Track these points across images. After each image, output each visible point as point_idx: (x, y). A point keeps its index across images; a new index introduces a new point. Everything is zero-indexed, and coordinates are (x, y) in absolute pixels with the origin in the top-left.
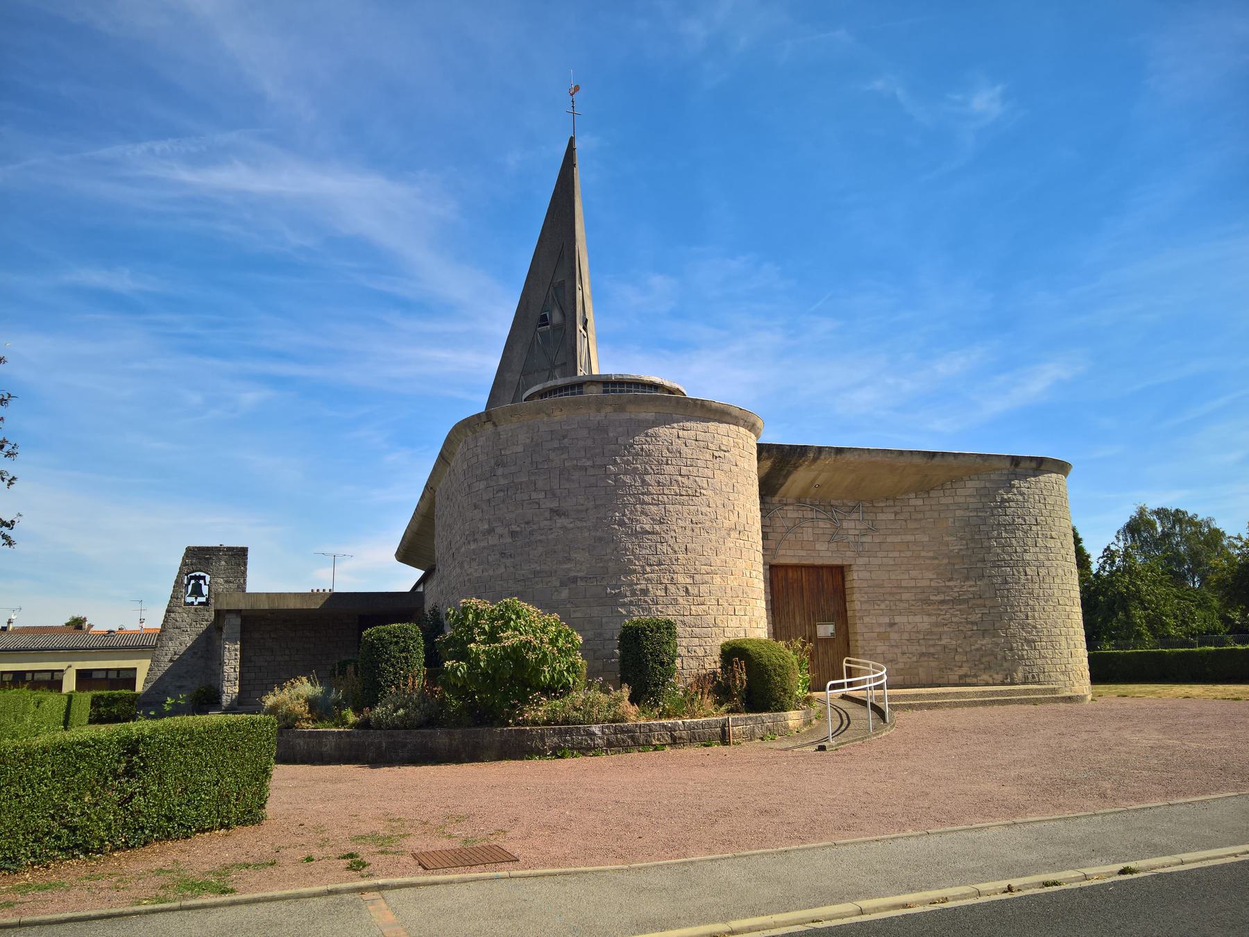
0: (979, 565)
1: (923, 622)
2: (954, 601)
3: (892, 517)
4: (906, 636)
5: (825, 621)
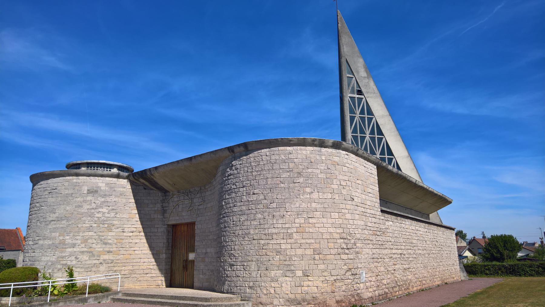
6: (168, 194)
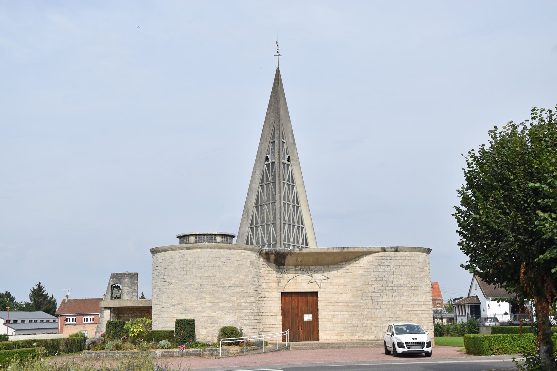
0: (367, 292)
1: (346, 314)
4: (339, 320)
5: (308, 313)
6: (282, 267)
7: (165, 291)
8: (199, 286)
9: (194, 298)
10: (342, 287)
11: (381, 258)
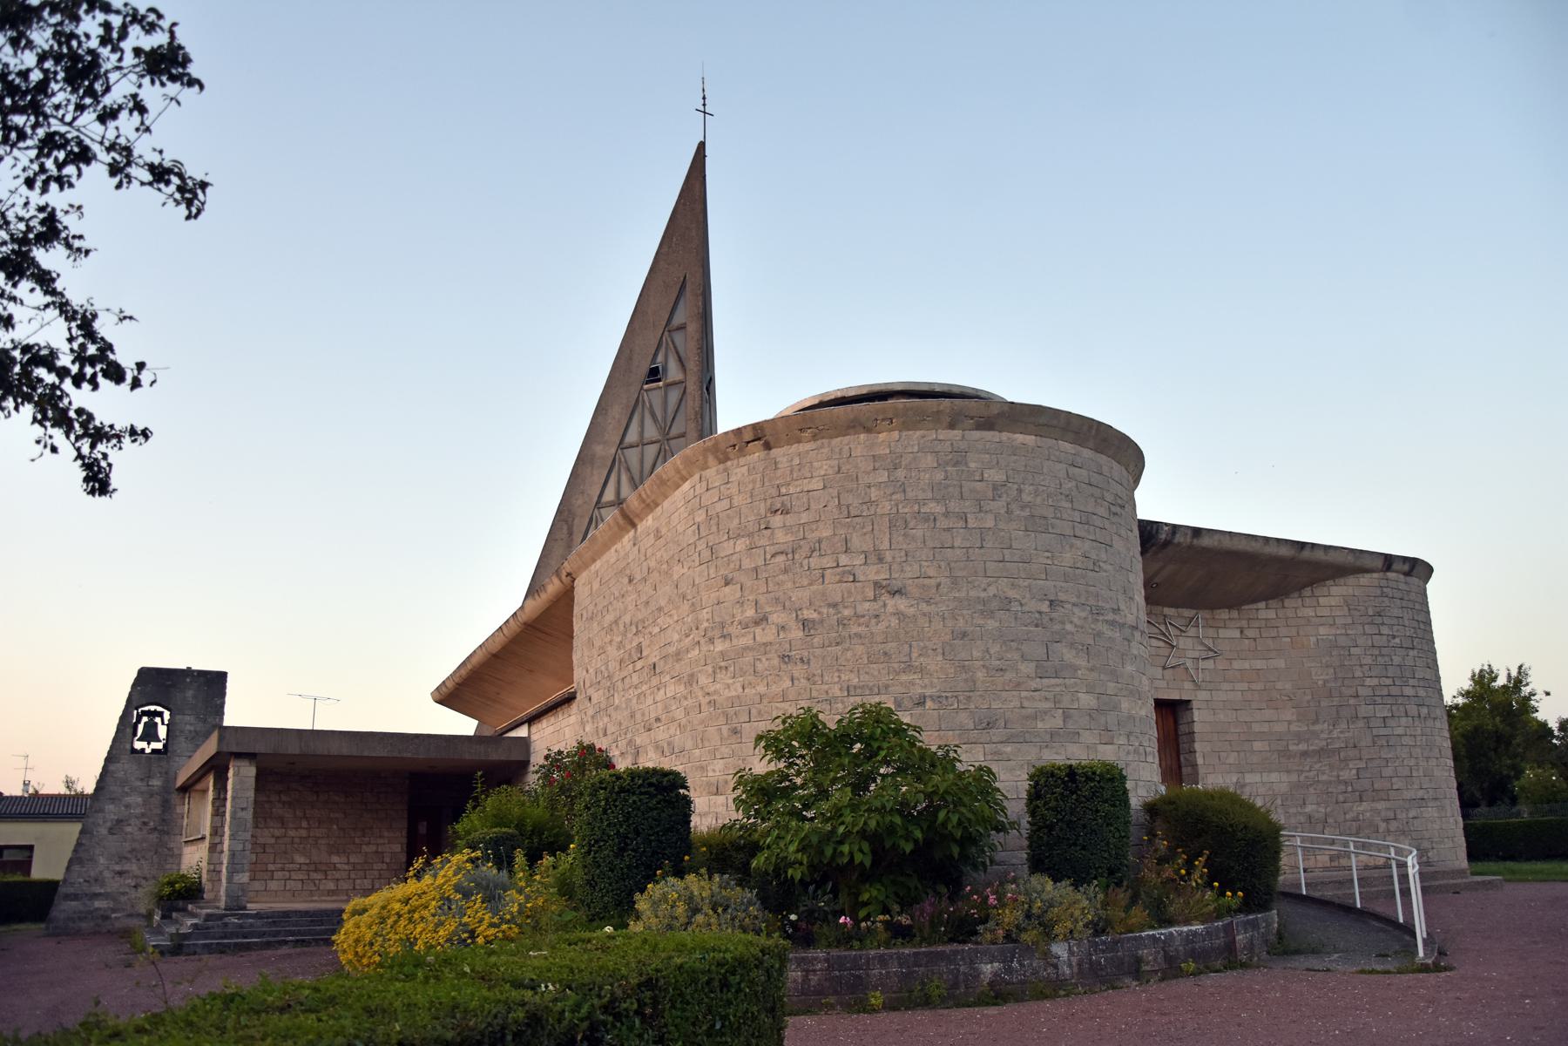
0: (1352, 701)
2: (1321, 753)
3: (1237, 634)
7: (855, 629)
8: (1045, 607)
9: (1027, 668)
10: (1259, 686)
11: (1378, 592)
